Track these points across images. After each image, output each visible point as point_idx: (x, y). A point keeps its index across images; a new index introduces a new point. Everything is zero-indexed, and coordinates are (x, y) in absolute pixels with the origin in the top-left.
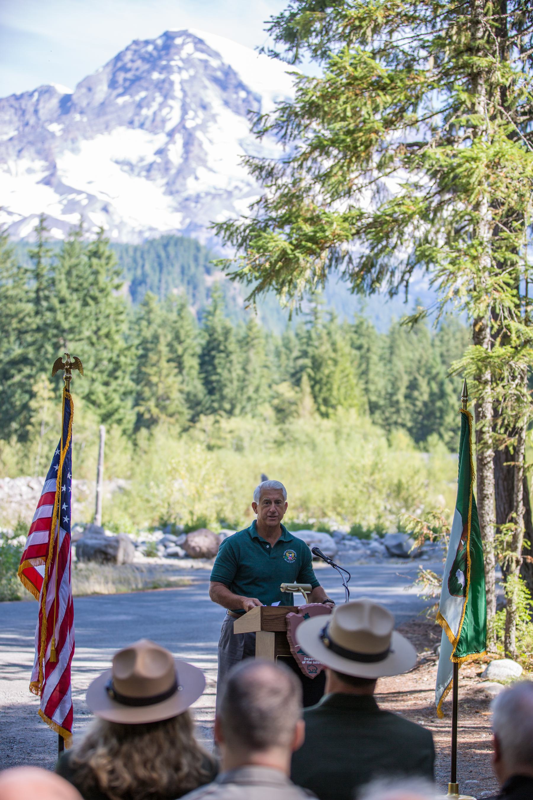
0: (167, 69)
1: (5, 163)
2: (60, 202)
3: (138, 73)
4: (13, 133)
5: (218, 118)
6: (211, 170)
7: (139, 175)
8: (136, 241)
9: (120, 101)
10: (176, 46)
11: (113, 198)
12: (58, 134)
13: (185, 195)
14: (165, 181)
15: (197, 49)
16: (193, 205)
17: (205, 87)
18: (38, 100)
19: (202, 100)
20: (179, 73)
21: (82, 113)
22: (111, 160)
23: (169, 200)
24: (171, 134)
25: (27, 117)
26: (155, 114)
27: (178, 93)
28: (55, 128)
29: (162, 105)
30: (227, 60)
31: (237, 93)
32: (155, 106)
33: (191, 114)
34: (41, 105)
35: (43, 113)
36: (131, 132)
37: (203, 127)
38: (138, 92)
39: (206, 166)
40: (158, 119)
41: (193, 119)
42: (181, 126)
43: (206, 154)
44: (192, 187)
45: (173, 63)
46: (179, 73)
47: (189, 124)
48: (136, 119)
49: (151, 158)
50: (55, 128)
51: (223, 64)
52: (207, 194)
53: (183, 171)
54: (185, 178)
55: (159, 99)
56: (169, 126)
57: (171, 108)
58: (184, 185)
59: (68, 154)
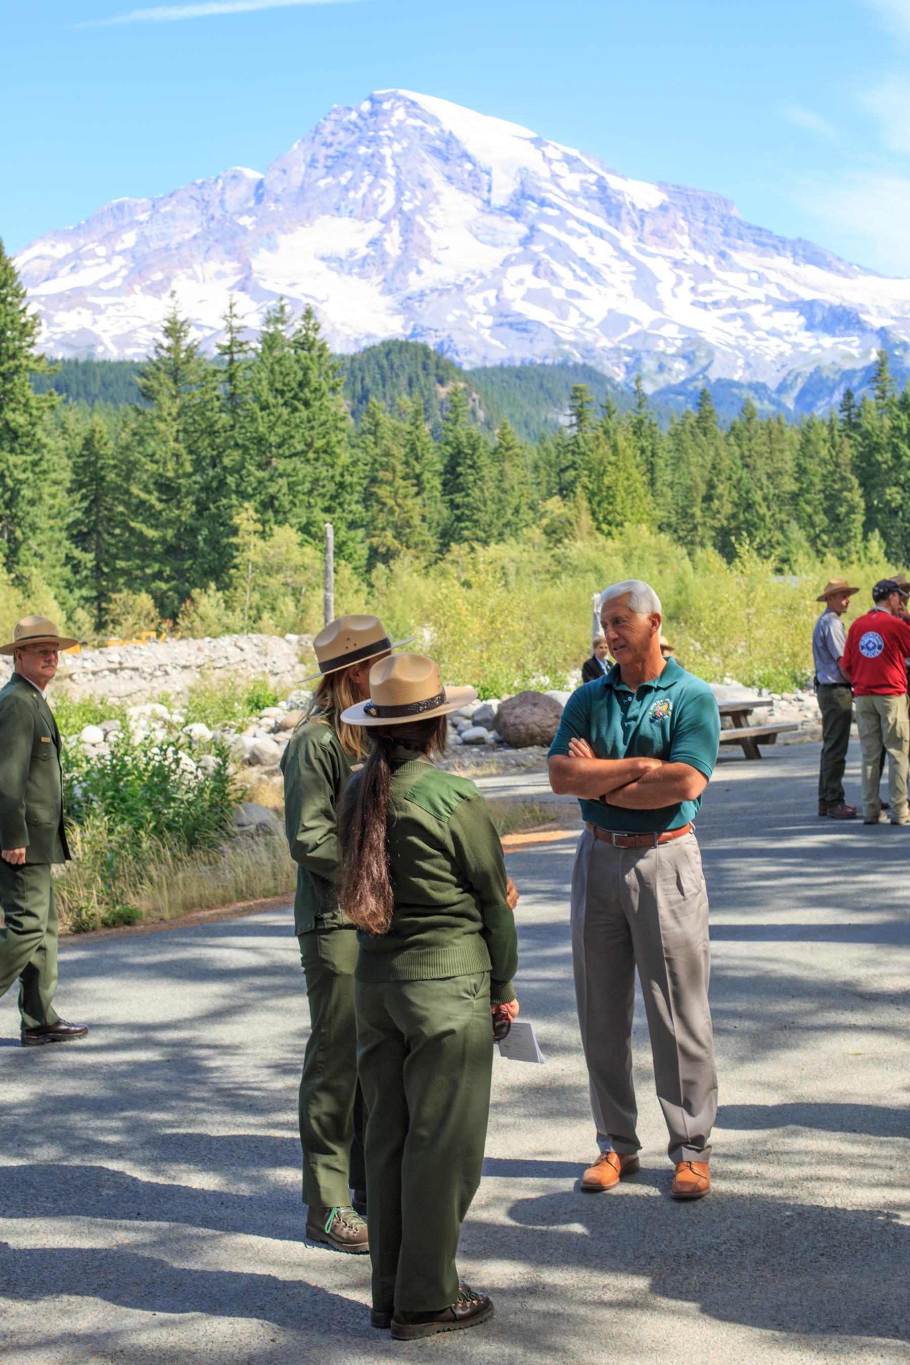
1: (190, 267)
2: (258, 311)
3: (340, 148)
4: (196, 230)
5: (441, 198)
7: (350, 273)
8: (351, 350)
9: (322, 183)
10: (385, 113)
11: (322, 302)
12: (250, 228)
13: (407, 292)
14: (381, 277)
15: (409, 115)
16: (417, 304)
17: (423, 161)
18: (223, 189)
19: (419, 176)
20: (390, 146)
21: (277, 200)
22: (315, 256)
23: (388, 300)
25: (212, 210)
26: (365, 196)
27: (391, 171)
28: (246, 221)
29: (372, 186)
30: (447, 126)
31: (461, 166)
32: (364, 188)
33: (408, 194)
34: (228, 194)
35: (232, 204)
36: (337, 221)
37: (422, 210)
38: (342, 172)
39: (429, 257)
40: (369, 203)
41: (410, 201)
42: (398, 210)
43: (429, 242)
44: (415, 283)
45: (382, 133)
46: (390, 146)
47: (407, 207)
48: (343, 204)
49: (363, 251)
50: (246, 221)
51: (442, 130)
52: (433, 290)
53: (405, 264)
54: (405, 273)
55: (369, 179)
56: (383, 210)
57: (384, 188)
58: (405, 282)
59: (264, 253)
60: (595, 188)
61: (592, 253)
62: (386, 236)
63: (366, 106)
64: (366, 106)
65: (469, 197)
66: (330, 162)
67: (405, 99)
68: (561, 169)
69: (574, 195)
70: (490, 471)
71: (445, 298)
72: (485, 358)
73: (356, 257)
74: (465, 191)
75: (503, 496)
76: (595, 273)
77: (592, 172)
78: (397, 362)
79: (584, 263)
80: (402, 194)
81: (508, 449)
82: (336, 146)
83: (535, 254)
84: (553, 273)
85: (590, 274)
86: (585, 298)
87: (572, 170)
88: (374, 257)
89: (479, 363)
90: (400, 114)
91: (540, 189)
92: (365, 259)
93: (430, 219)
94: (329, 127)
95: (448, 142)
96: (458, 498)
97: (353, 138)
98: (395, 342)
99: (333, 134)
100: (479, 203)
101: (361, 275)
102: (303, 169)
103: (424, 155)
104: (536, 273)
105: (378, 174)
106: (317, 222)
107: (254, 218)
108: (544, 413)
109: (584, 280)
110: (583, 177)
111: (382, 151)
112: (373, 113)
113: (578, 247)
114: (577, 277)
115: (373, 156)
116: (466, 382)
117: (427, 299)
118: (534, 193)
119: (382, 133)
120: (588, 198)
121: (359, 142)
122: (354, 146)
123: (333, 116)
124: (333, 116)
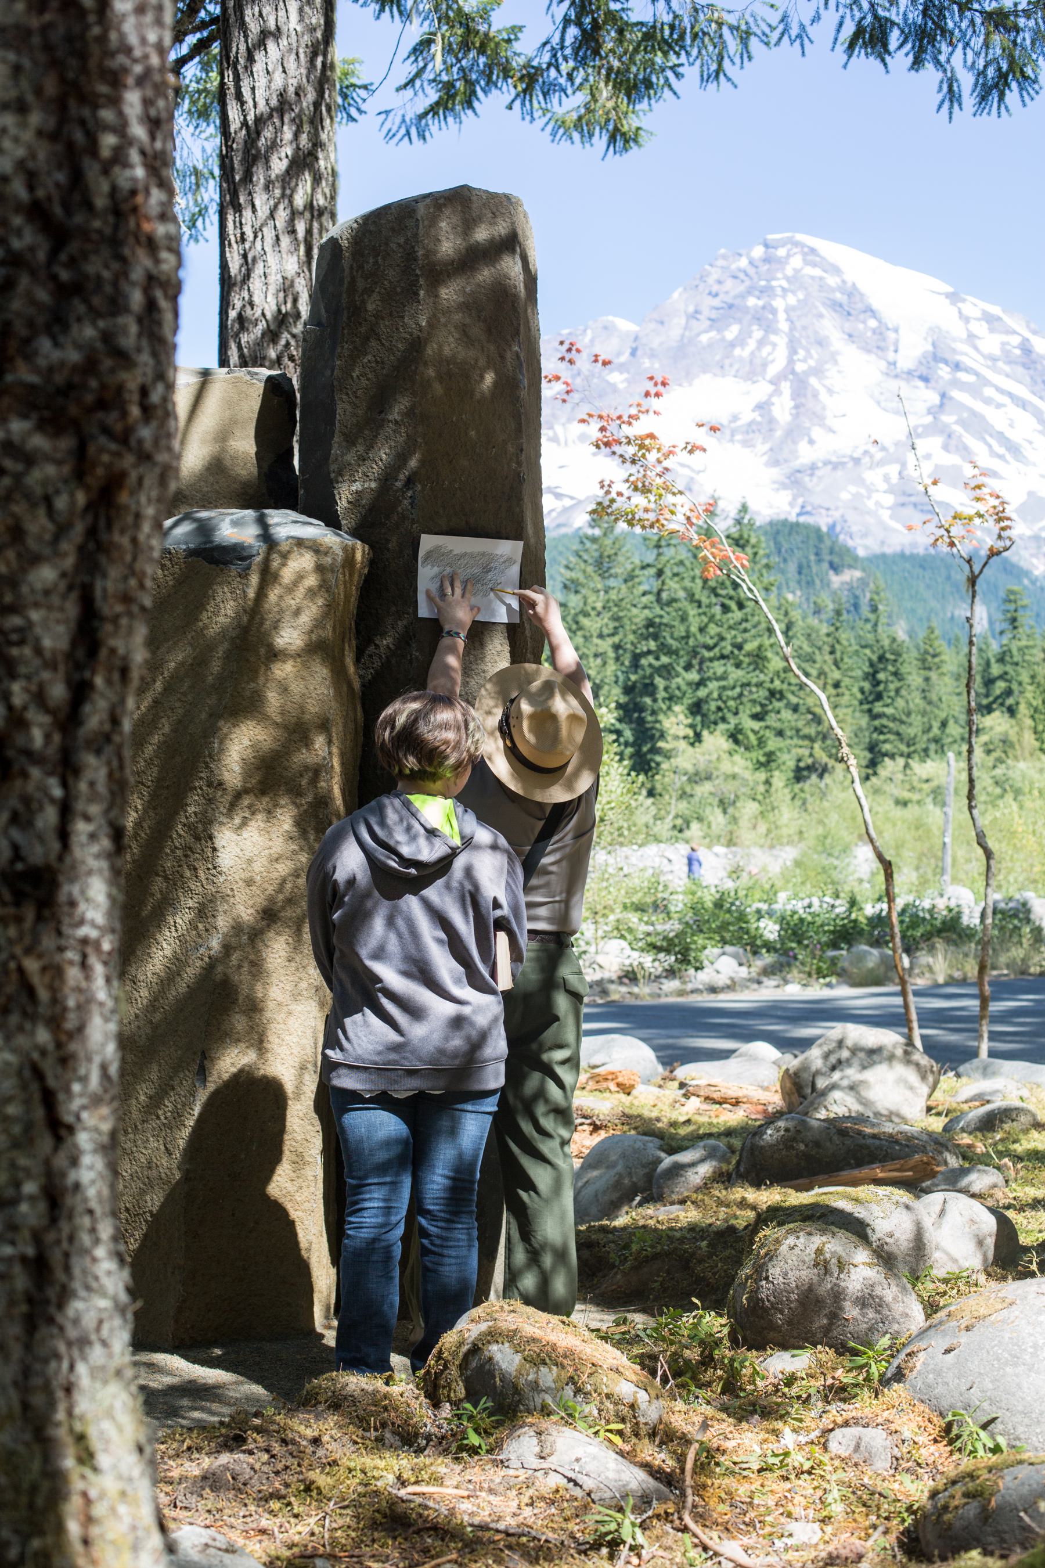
0: (767, 291)
5: (839, 358)
6: (831, 430)
7: (732, 441)
9: (704, 338)
12: (621, 386)
13: (797, 464)
14: (767, 447)
15: (806, 262)
16: (807, 479)
17: (821, 316)
20: (784, 297)
23: (775, 473)
24: (775, 382)
26: (752, 353)
27: (783, 325)
29: (761, 343)
30: (849, 278)
31: (864, 322)
32: (752, 344)
33: (802, 353)
37: (817, 371)
38: (728, 326)
39: (822, 425)
41: (804, 361)
42: (790, 370)
43: (824, 408)
44: (805, 454)
45: (774, 283)
46: (784, 297)
47: (800, 367)
48: (727, 362)
49: (748, 416)
51: (844, 282)
52: (826, 463)
53: (795, 432)
54: (795, 443)
55: (758, 334)
56: (772, 371)
60: (1018, 352)
61: (1011, 426)
62: (774, 399)
63: (758, 252)
64: (758, 252)
65: (872, 358)
66: (714, 315)
67: (802, 245)
68: (980, 328)
69: (994, 359)
70: (915, 679)
71: (839, 473)
72: (883, 543)
73: (739, 423)
74: (869, 351)
75: (928, 708)
76: (1014, 449)
77: (1015, 332)
78: (786, 546)
79: (1001, 437)
80: (796, 353)
81: (934, 656)
82: (722, 296)
83: (946, 426)
84: (966, 448)
85: (1008, 449)
86: (1001, 478)
87: (992, 330)
88: (759, 424)
89: (877, 549)
90: (796, 262)
91: (954, 351)
92: (750, 424)
93: (827, 382)
94: (715, 274)
95: (850, 295)
96: (878, 708)
97: (742, 288)
98: (785, 523)
99: (720, 282)
100: (883, 365)
101: (747, 444)
102: (683, 321)
103: (822, 310)
104: (946, 448)
105: (770, 328)
106: (696, 382)
107: (625, 376)
108: (950, 608)
109: (1001, 457)
110: (1005, 338)
111: (775, 303)
112: (767, 260)
113: (996, 418)
114: (993, 454)
115: (764, 308)
116: (864, 570)
117: (818, 473)
118: (947, 356)
119: (774, 283)
120: (1009, 362)
121: (749, 292)
122: (743, 296)
123: (720, 263)
124: (720, 263)
